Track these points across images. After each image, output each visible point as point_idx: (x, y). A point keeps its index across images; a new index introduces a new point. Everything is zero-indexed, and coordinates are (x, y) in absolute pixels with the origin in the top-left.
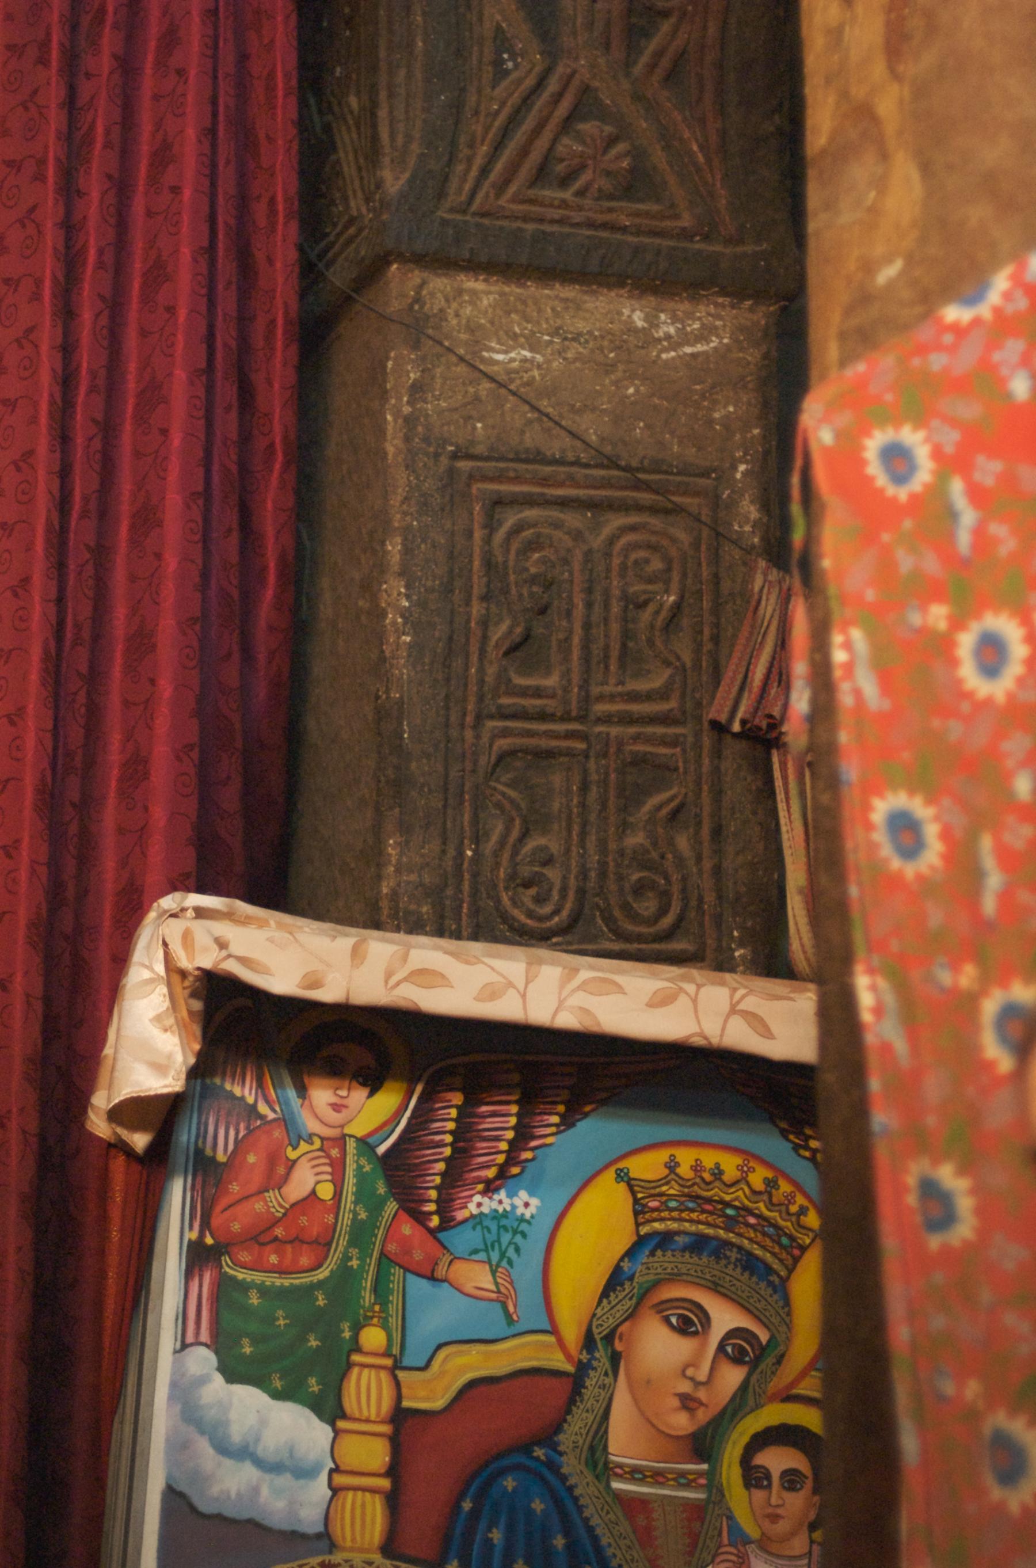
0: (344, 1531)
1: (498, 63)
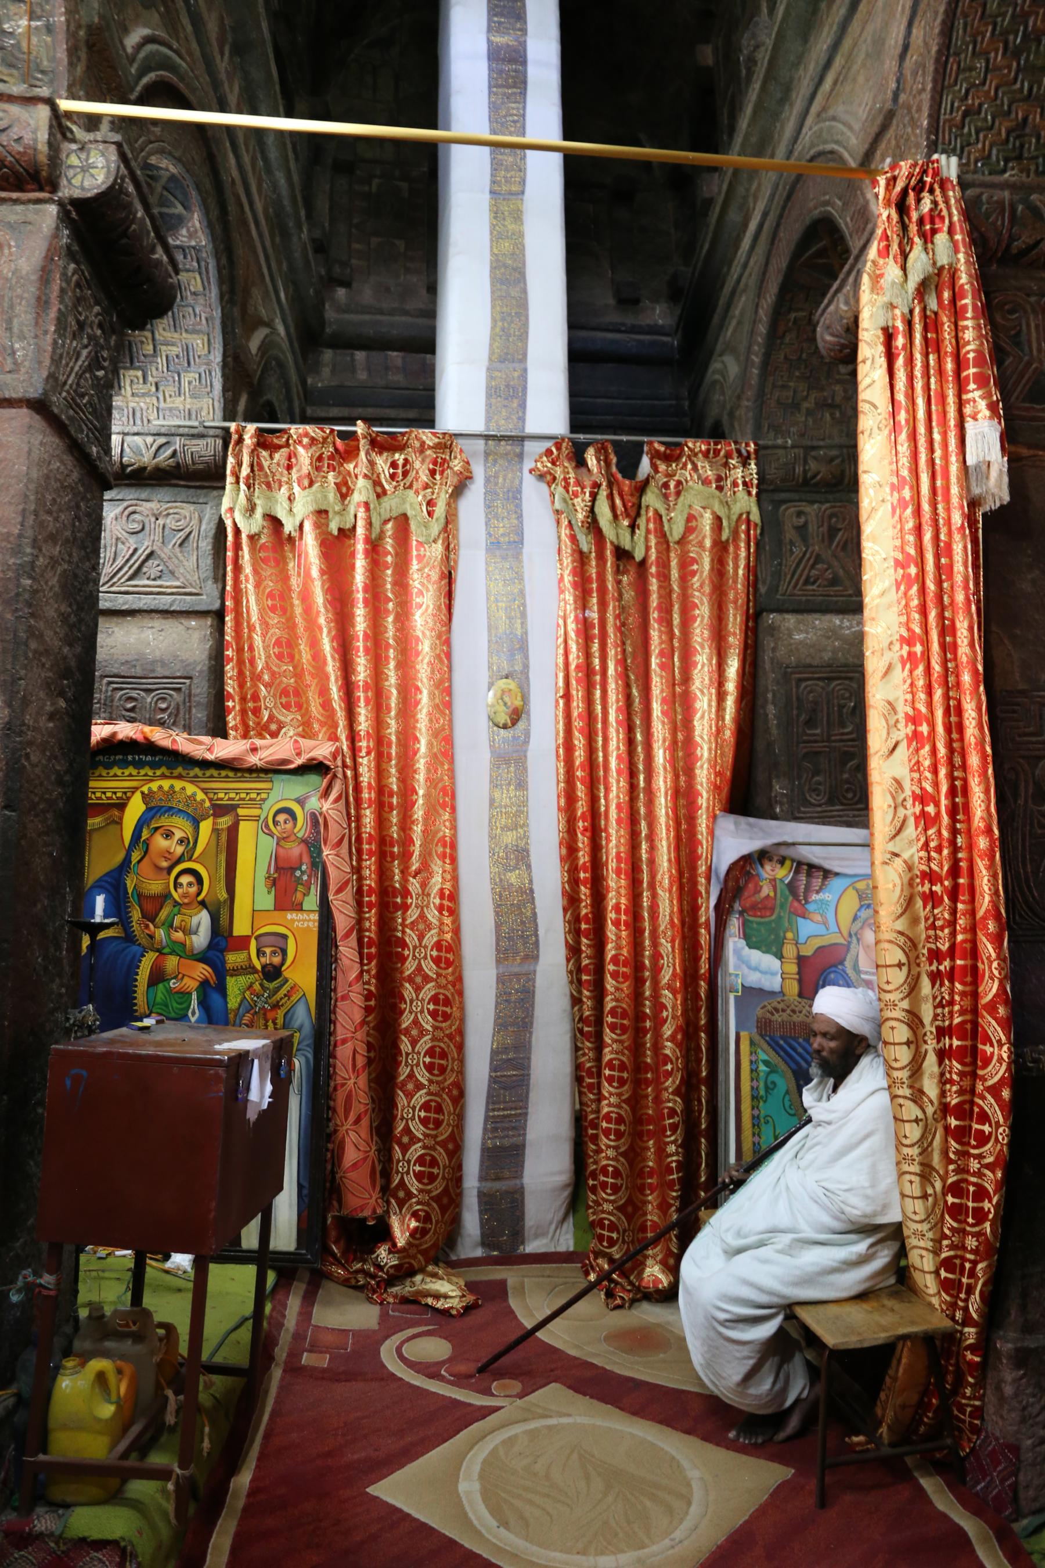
0: (787, 990)
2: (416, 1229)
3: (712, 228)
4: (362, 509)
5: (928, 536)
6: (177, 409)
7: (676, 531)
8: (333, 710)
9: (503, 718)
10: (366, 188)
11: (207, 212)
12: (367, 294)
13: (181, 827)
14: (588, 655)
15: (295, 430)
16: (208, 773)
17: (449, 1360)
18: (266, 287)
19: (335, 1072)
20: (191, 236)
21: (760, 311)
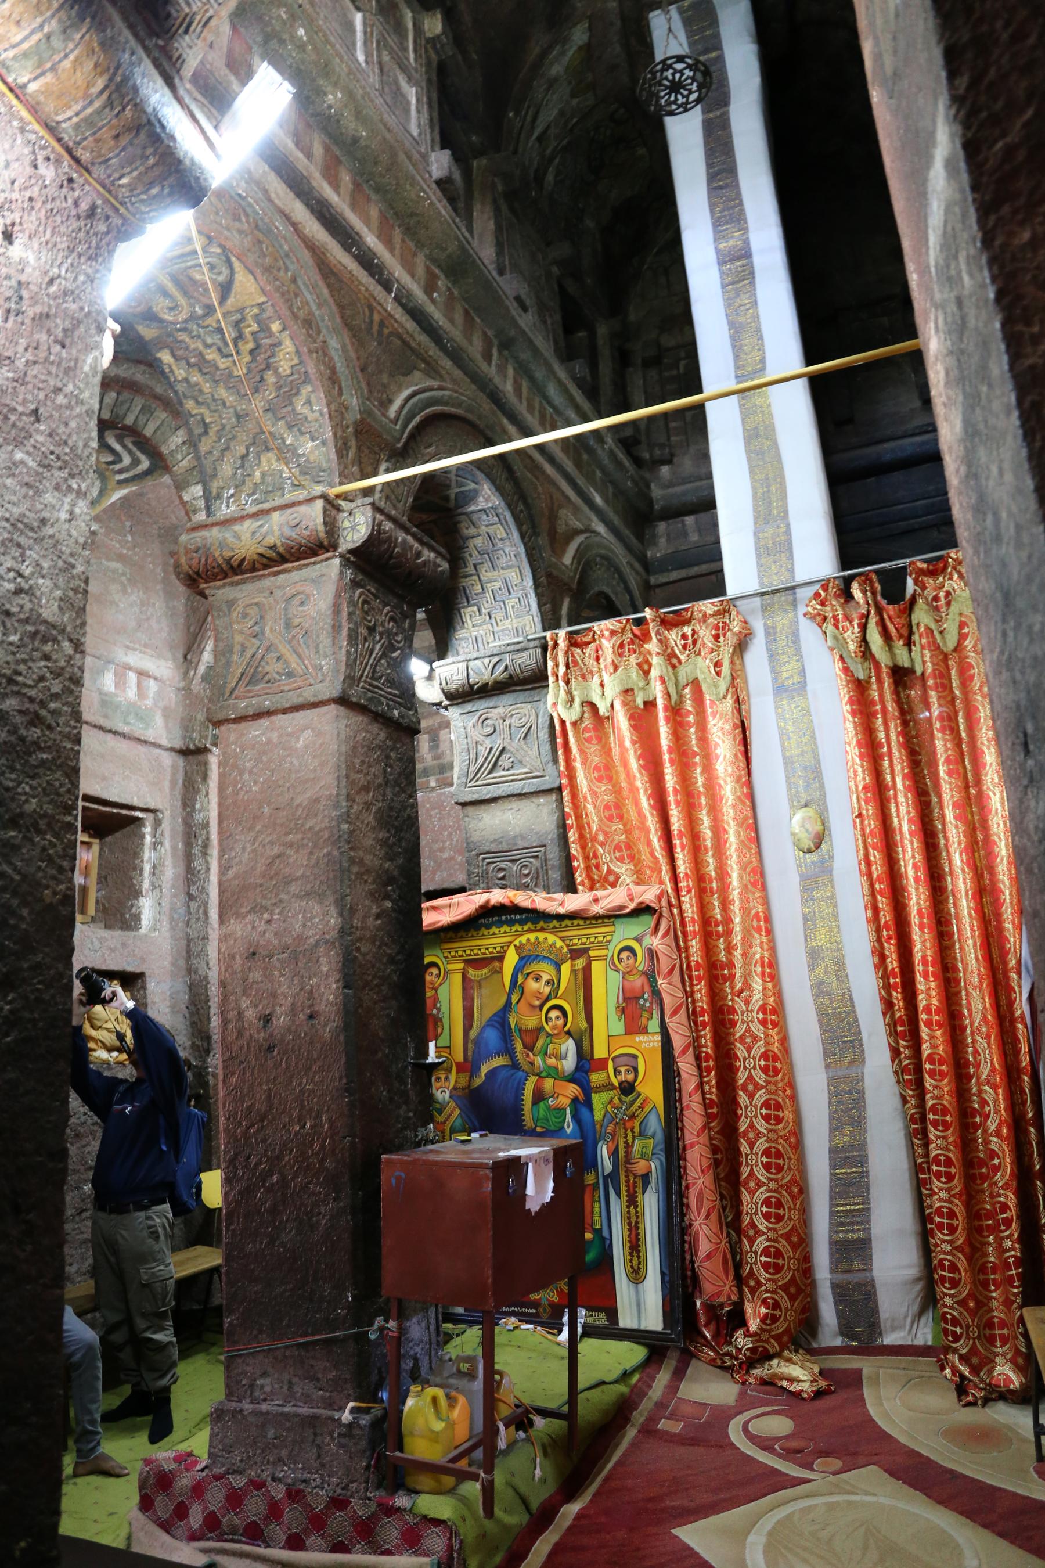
2: (766, 1315)
4: (658, 683)
9: (808, 843)
10: (674, 372)
11: (493, 481)
13: (546, 970)
15: (598, 626)
16: (564, 924)
17: (787, 1437)
19: (686, 1173)
20: (487, 500)
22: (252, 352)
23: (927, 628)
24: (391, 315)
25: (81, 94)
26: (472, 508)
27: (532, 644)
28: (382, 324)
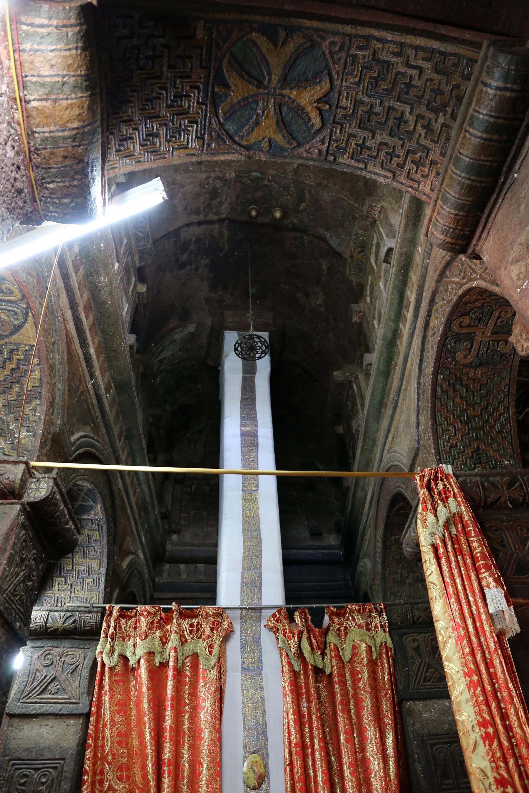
1: (413, 662)
3: (351, 499)
4: (173, 651)
5: (479, 656)
6: (80, 597)
7: (347, 655)
8: (148, 780)
9: (253, 782)
10: (189, 490)
11: (104, 504)
12: (187, 537)
14: (302, 735)
15: (140, 608)
18: (134, 536)
21: (378, 537)
22: (12, 370)
23: (335, 645)
24: (89, 392)
25: (61, 122)
26: (85, 517)
27: (96, 610)
28: (82, 393)
